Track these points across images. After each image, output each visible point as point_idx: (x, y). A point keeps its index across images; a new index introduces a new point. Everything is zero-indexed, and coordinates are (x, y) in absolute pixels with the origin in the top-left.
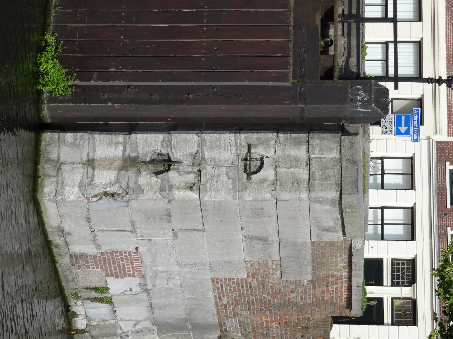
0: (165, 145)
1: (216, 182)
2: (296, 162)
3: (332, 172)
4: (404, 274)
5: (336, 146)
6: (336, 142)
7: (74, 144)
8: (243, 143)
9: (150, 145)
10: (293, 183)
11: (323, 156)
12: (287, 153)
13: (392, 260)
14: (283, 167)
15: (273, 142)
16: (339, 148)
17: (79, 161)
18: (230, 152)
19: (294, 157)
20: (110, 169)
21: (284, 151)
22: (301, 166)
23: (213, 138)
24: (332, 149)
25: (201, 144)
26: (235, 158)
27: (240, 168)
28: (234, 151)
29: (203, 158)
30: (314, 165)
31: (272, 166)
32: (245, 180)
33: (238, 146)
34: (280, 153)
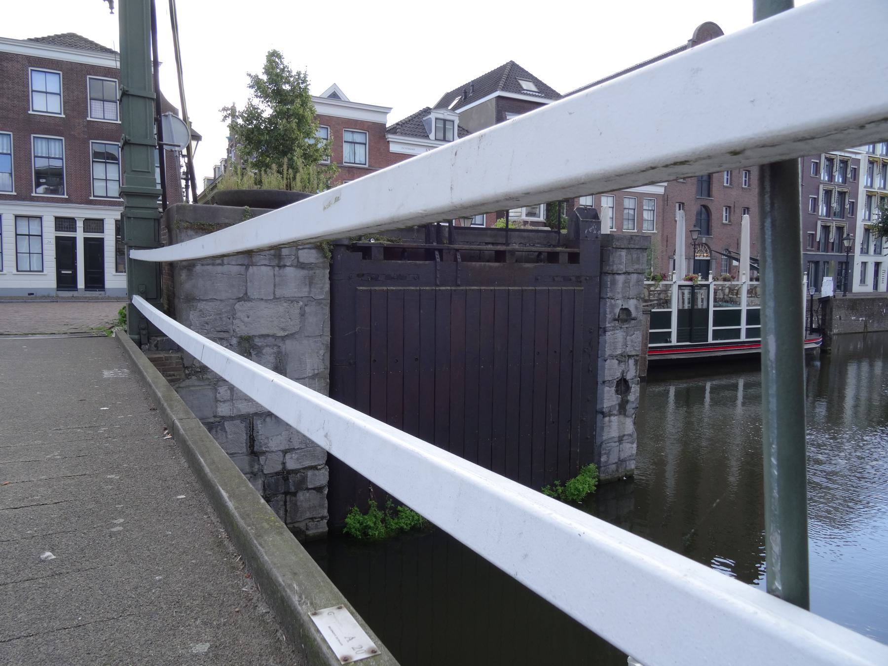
0: (612, 385)
1: (635, 343)
2: (626, 282)
3: (635, 256)
4: (66, 224)
5: (618, 253)
7: (608, 454)
9: (612, 396)
10: (639, 285)
11: (624, 262)
13: (56, 231)
14: (629, 293)
15: (613, 301)
16: (620, 250)
17: (618, 447)
18: (618, 334)
19: (623, 285)
20: (624, 423)
21: (619, 293)
22: (629, 279)
23: (608, 348)
24: (620, 255)
25: (612, 357)
26: (622, 330)
28: (618, 331)
29: (621, 355)
30: (630, 270)
31: (627, 301)
32: (635, 321)
33: (614, 328)
34: (620, 296)
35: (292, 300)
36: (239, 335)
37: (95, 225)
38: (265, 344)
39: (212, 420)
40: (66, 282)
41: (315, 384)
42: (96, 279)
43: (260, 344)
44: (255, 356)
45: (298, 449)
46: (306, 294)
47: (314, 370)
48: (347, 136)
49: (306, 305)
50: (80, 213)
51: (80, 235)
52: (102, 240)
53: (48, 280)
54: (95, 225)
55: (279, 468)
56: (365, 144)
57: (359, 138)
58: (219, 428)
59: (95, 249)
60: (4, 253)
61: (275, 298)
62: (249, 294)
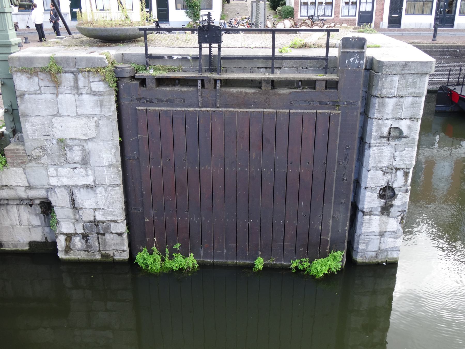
0: (375, 191)
1: (406, 158)
2: (398, 106)
5: (389, 78)
6: (386, 77)
7: (367, 244)
8: (379, 141)
9: (374, 200)
10: (414, 107)
11: (397, 87)
12: (390, 112)
14: (401, 114)
15: (380, 121)
16: (392, 75)
17: (379, 240)
18: (385, 150)
19: (394, 107)
21: (388, 114)
22: (402, 102)
23: (372, 161)
24: (392, 80)
25: (376, 168)
26: (390, 146)
27: (397, 143)
31: (399, 121)
32: (407, 139)
33: (381, 144)
34: (390, 117)
35: (89, 117)
36: (57, 138)
38: (74, 144)
39: (47, 187)
41: (111, 170)
43: (71, 144)
44: (68, 151)
45: (103, 209)
46: (99, 113)
47: (109, 162)
49: (99, 120)
55: (92, 219)
58: (52, 192)
61: (77, 115)
62: (60, 112)
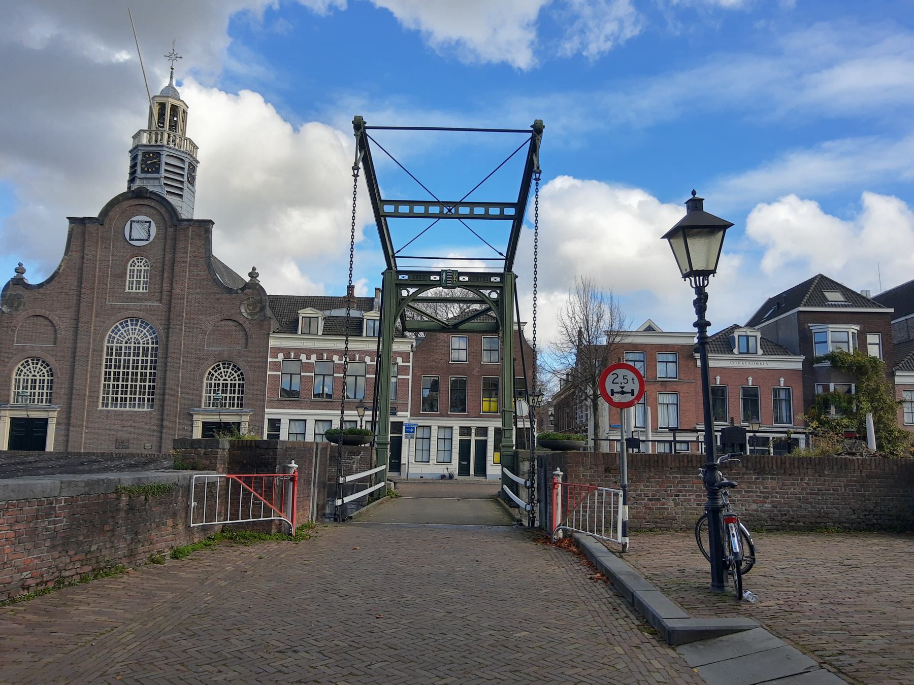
37: (483, 431)
40: (464, 470)
42: (481, 469)
48: (660, 357)
50: (474, 424)
51: (473, 438)
52: (486, 441)
53: (454, 467)
54: (483, 431)
56: (676, 362)
57: (671, 358)
59: (482, 447)
60: (431, 450)
